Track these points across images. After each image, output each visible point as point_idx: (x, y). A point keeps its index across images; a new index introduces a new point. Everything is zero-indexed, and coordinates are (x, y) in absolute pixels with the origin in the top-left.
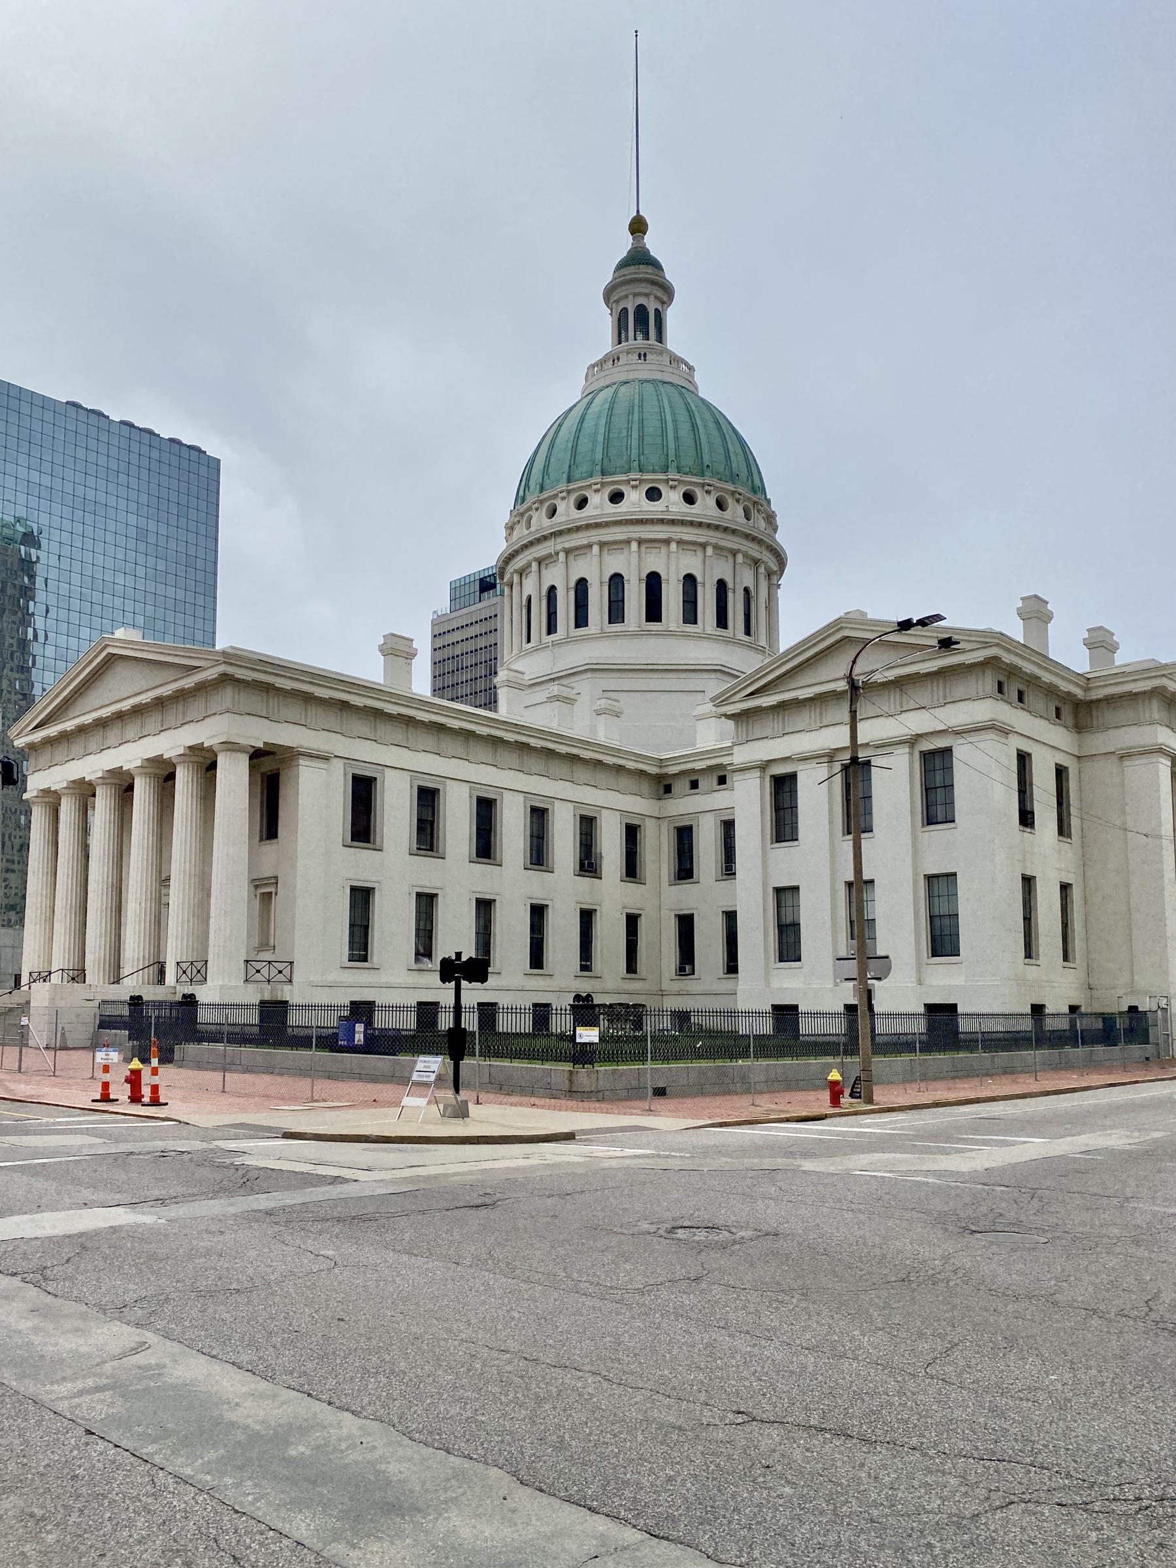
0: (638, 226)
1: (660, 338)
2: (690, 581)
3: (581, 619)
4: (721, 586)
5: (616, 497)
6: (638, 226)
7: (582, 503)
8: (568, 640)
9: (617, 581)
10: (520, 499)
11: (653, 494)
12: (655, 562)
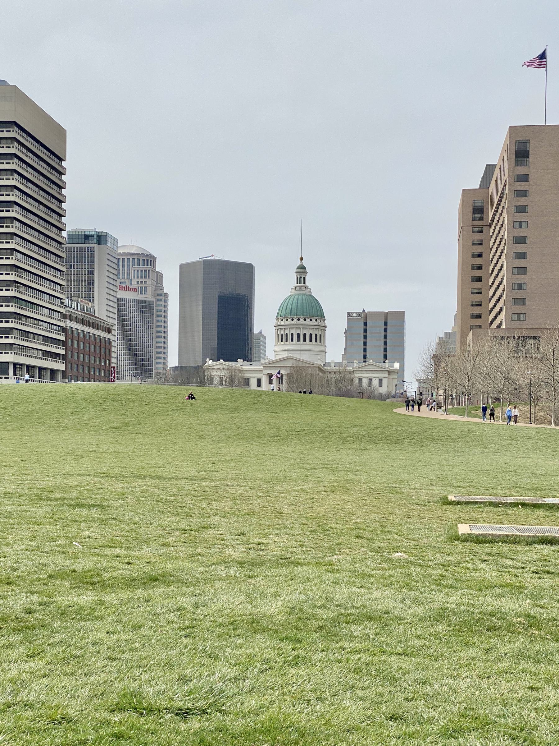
0: (302, 259)
1: (304, 283)
2: (305, 335)
3: (287, 341)
4: (311, 335)
5: (293, 320)
6: (302, 259)
7: (287, 320)
8: (284, 344)
9: (292, 334)
10: (278, 316)
11: (299, 320)
12: (298, 331)
